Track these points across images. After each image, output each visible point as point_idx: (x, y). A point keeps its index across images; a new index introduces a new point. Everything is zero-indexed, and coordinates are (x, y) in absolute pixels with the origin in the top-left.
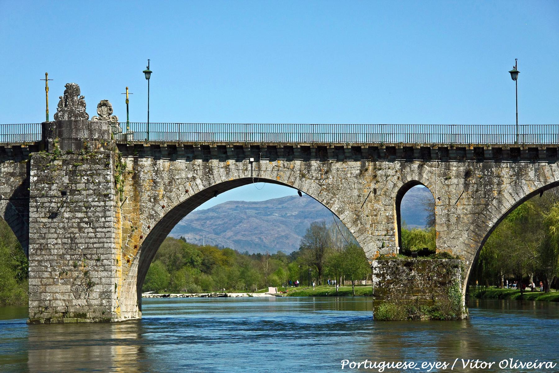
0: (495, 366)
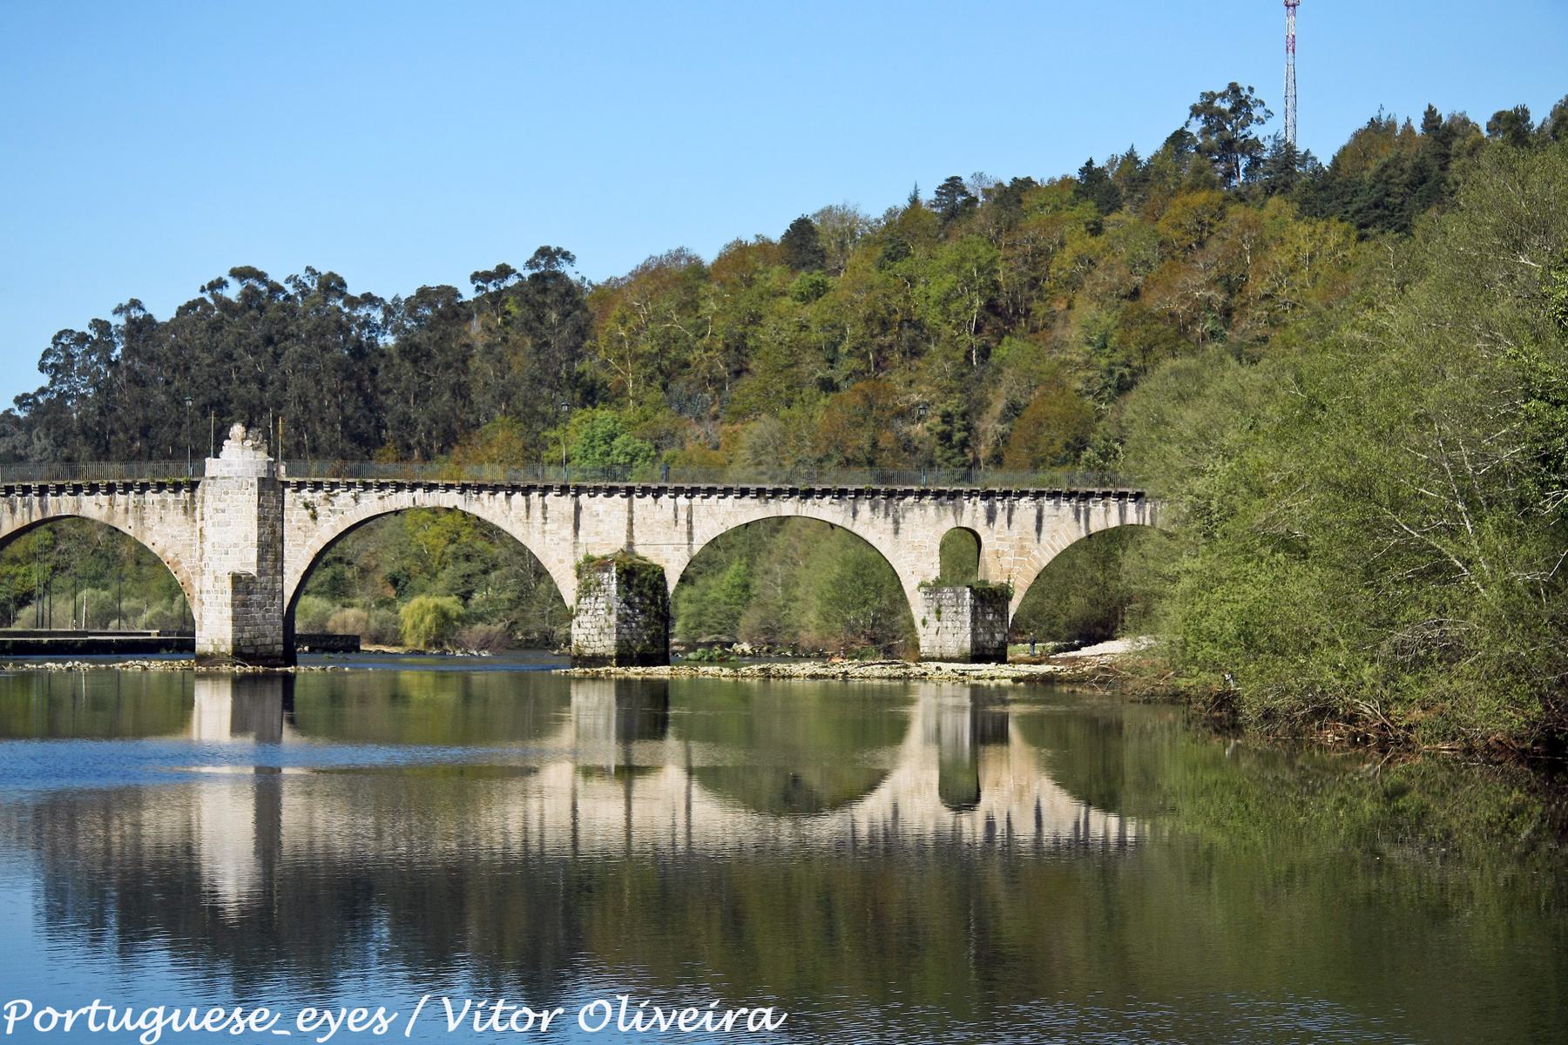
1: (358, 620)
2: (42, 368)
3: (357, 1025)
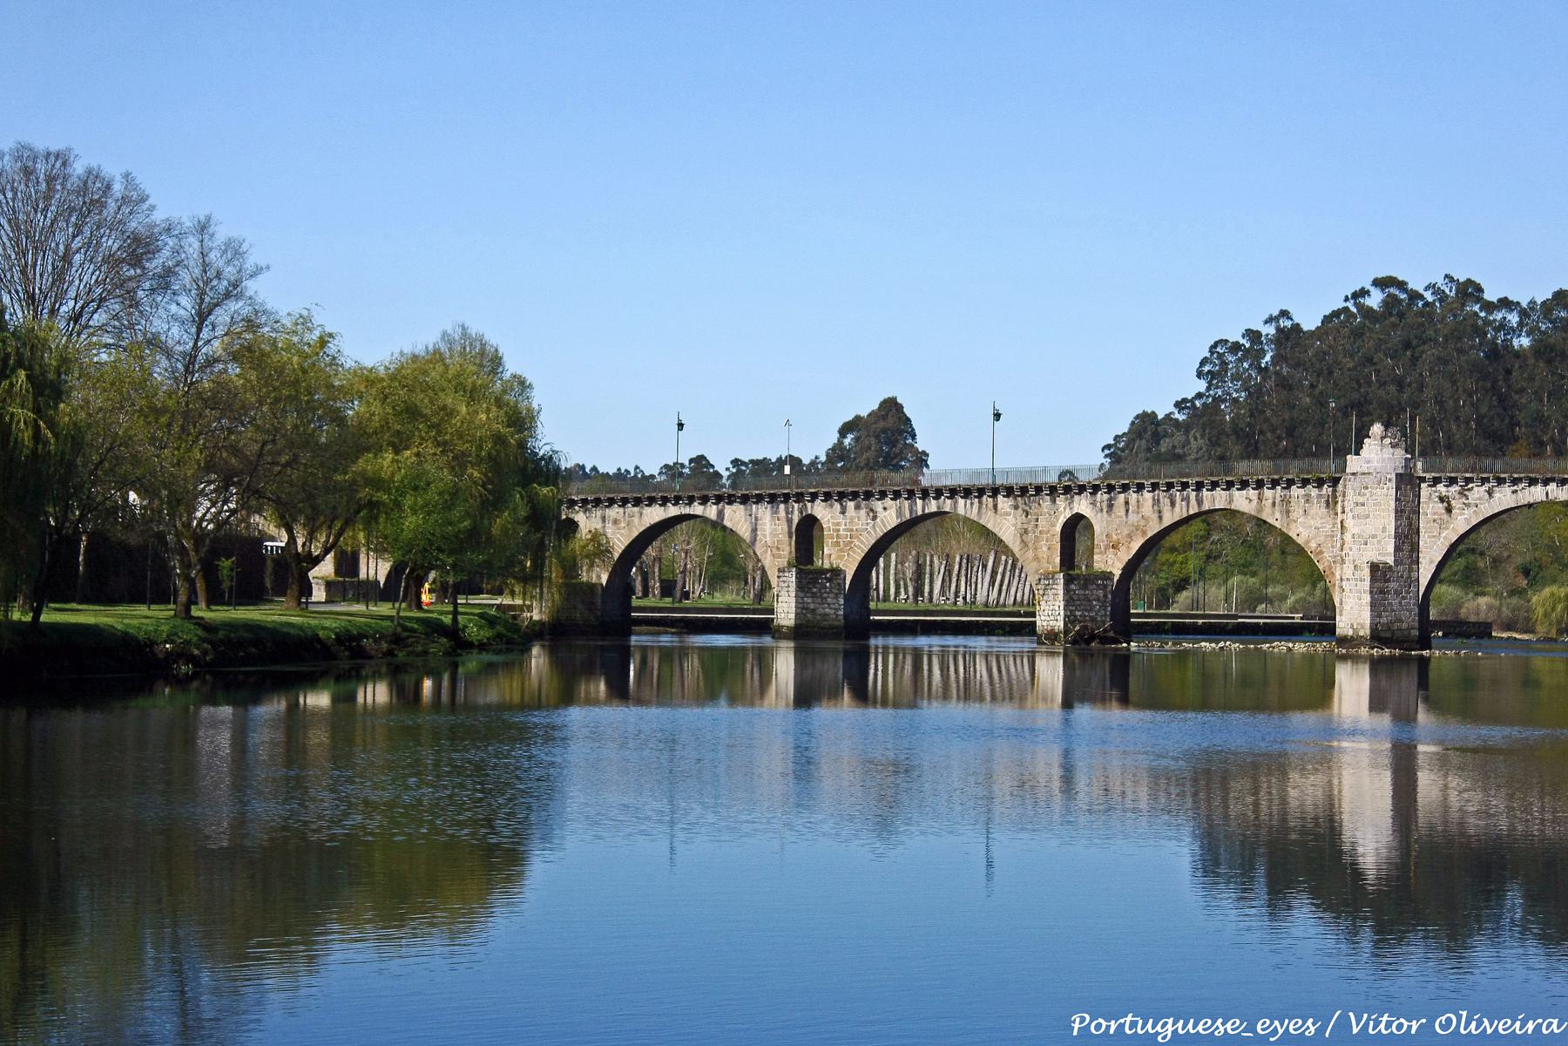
0: (1427, 1029)
1: (1490, 607)
2: (1200, 375)
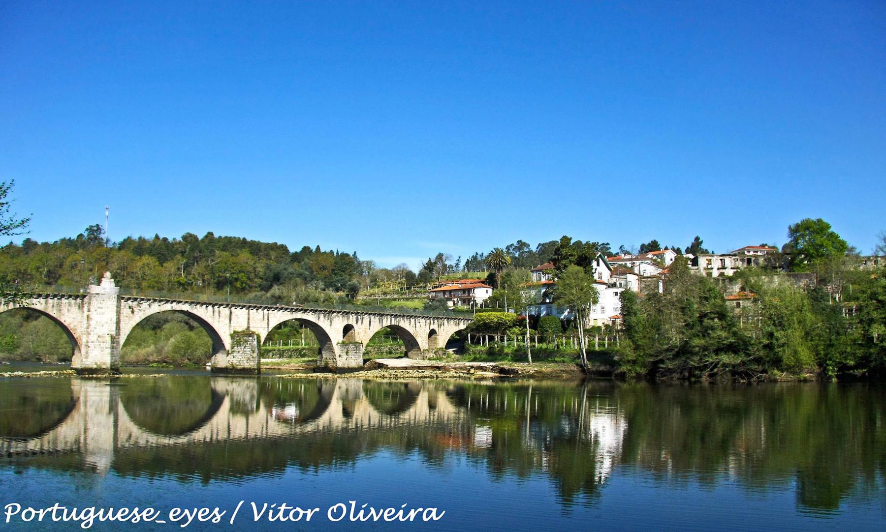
0: (320, 517)
3: (203, 517)
